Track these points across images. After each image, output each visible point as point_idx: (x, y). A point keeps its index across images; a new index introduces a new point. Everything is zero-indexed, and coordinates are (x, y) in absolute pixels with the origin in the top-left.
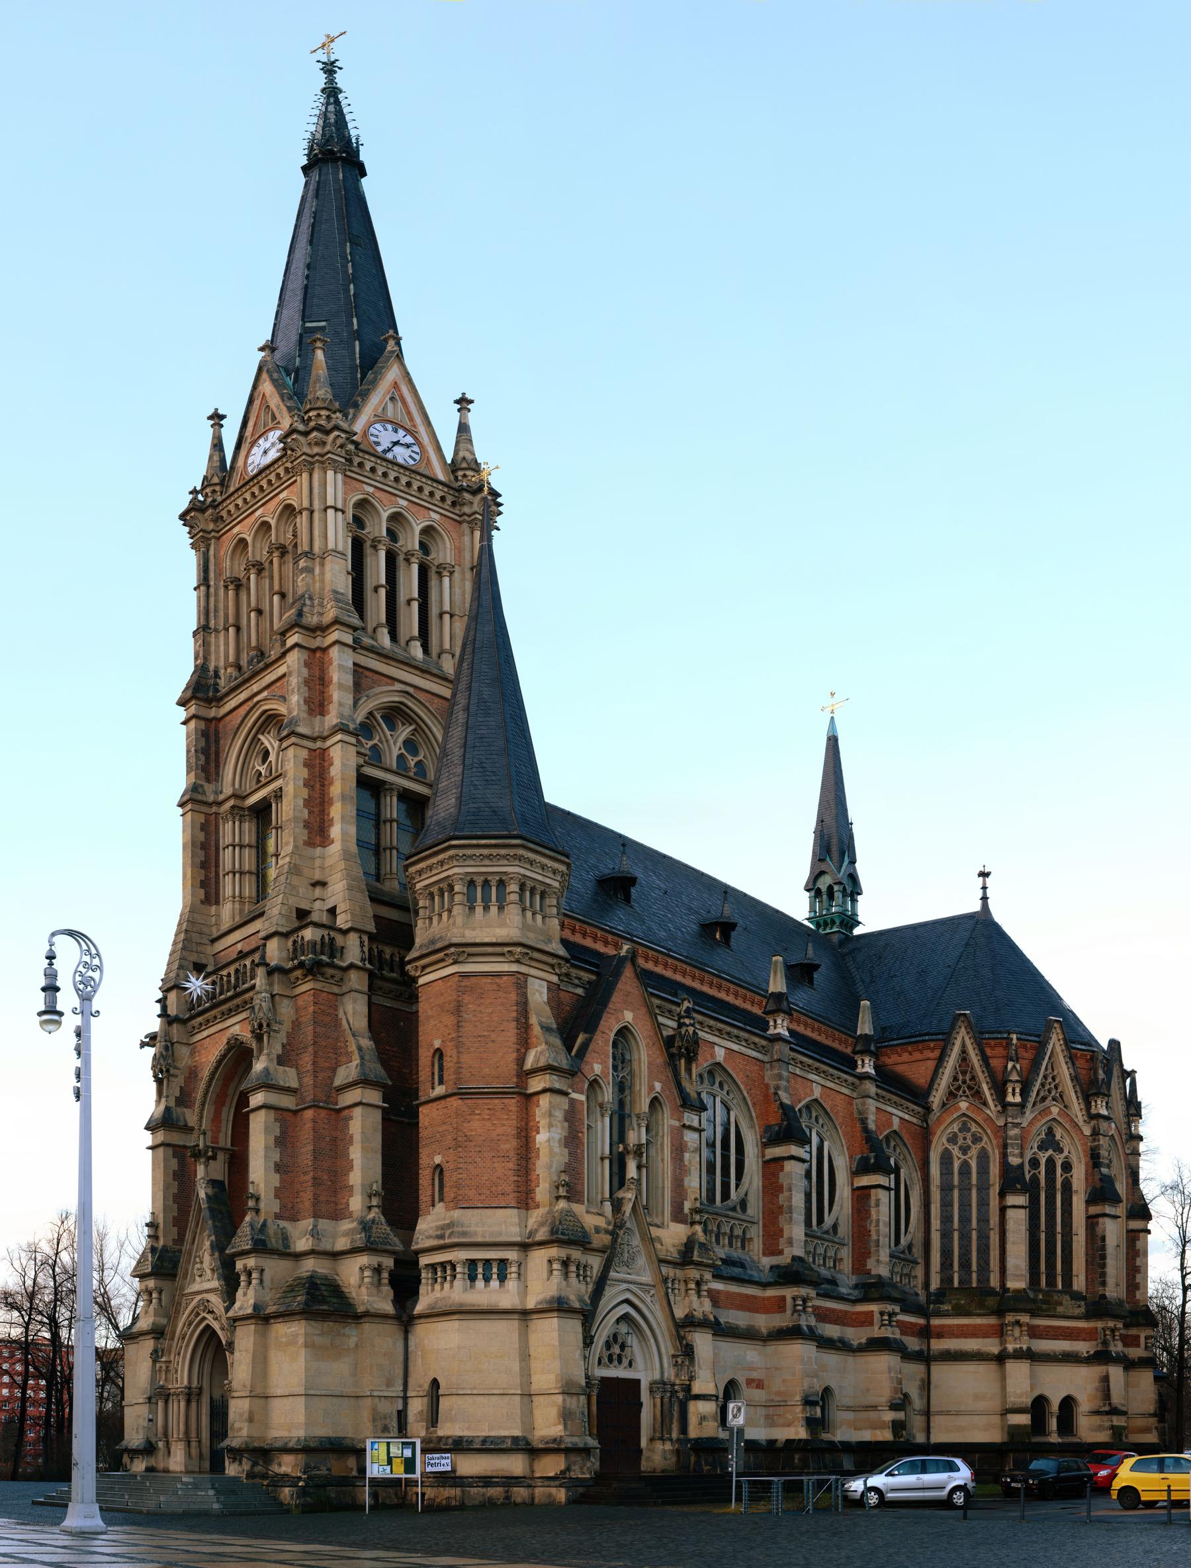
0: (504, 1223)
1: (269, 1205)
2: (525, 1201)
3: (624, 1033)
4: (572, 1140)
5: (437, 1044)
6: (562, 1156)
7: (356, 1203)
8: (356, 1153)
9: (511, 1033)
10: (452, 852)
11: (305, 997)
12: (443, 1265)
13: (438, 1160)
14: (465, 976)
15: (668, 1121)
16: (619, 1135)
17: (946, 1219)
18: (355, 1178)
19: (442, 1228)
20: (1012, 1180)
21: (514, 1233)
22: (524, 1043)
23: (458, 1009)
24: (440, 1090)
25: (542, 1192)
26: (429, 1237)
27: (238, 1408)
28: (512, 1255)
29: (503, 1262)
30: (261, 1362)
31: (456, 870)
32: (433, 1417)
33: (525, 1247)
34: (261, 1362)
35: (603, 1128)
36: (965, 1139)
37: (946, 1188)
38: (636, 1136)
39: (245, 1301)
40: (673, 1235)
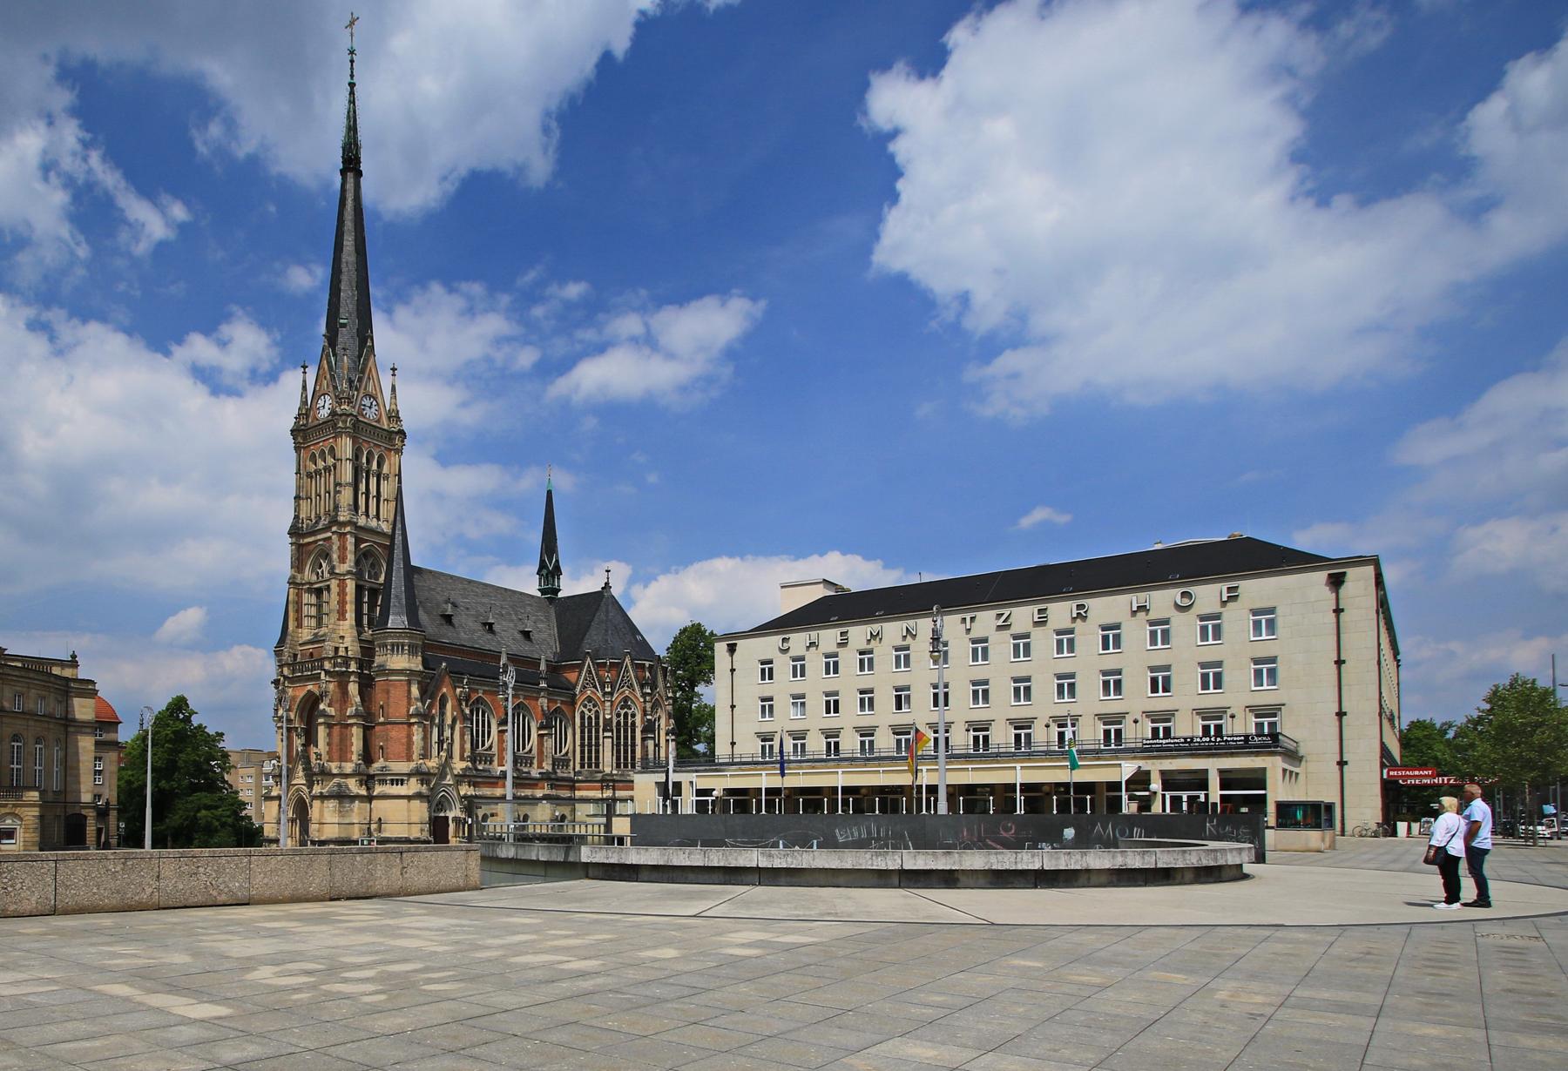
0: (402, 767)
1: (325, 757)
2: (409, 759)
3: (444, 696)
4: (425, 738)
6: (421, 744)
7: (354, 757)
8: (354, 740)
9: (405, 702)
15: (458, 726)
16: (441, 733)
17: (582, 738)
18: (354, 749)
20: (608, 723)
21: (406, 771)
22: (409, 704)
23: (388, 692)
25: (415, 756)
27: (313, 828)
30: (321, 812)
32: (380, 830)
33: (409, 775)
34: (321, 812)
35: (435, 730)
36: (590, 706)
37: (582, 725)
38: (447, 733)
39: (317, 790)
40: (459, 766)
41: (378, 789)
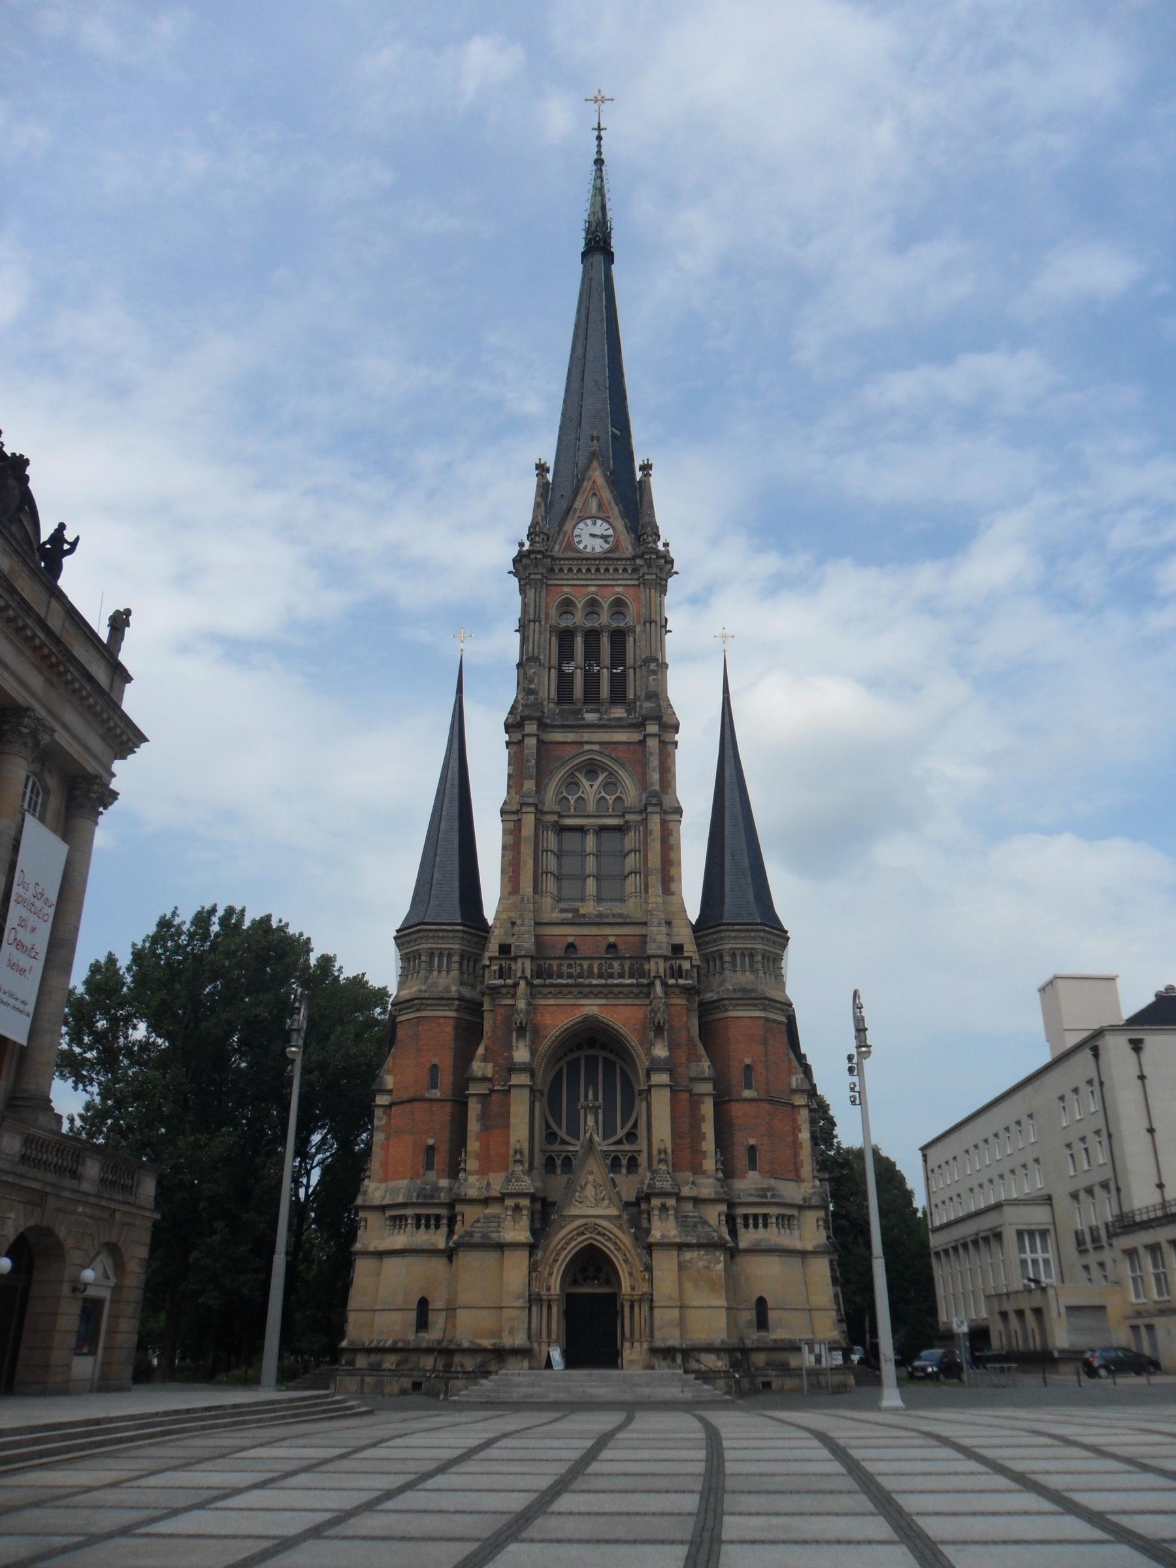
2: (798, 1179)
5: (748, 1061)
7: (709, 1164)
10: (762, 934)
11: (679, 1008)
12: (756, 1216)
13: (752, 1142)
14: (767, 1020)
19: (763, 1190)
23: (765, 1042)
24: (747, 1094)
26: (751, 1195)
28: (795, 1212)
29: (790, 1217)
31: (760, 946)
33: (800, 1208)
41: (747, 1237)
